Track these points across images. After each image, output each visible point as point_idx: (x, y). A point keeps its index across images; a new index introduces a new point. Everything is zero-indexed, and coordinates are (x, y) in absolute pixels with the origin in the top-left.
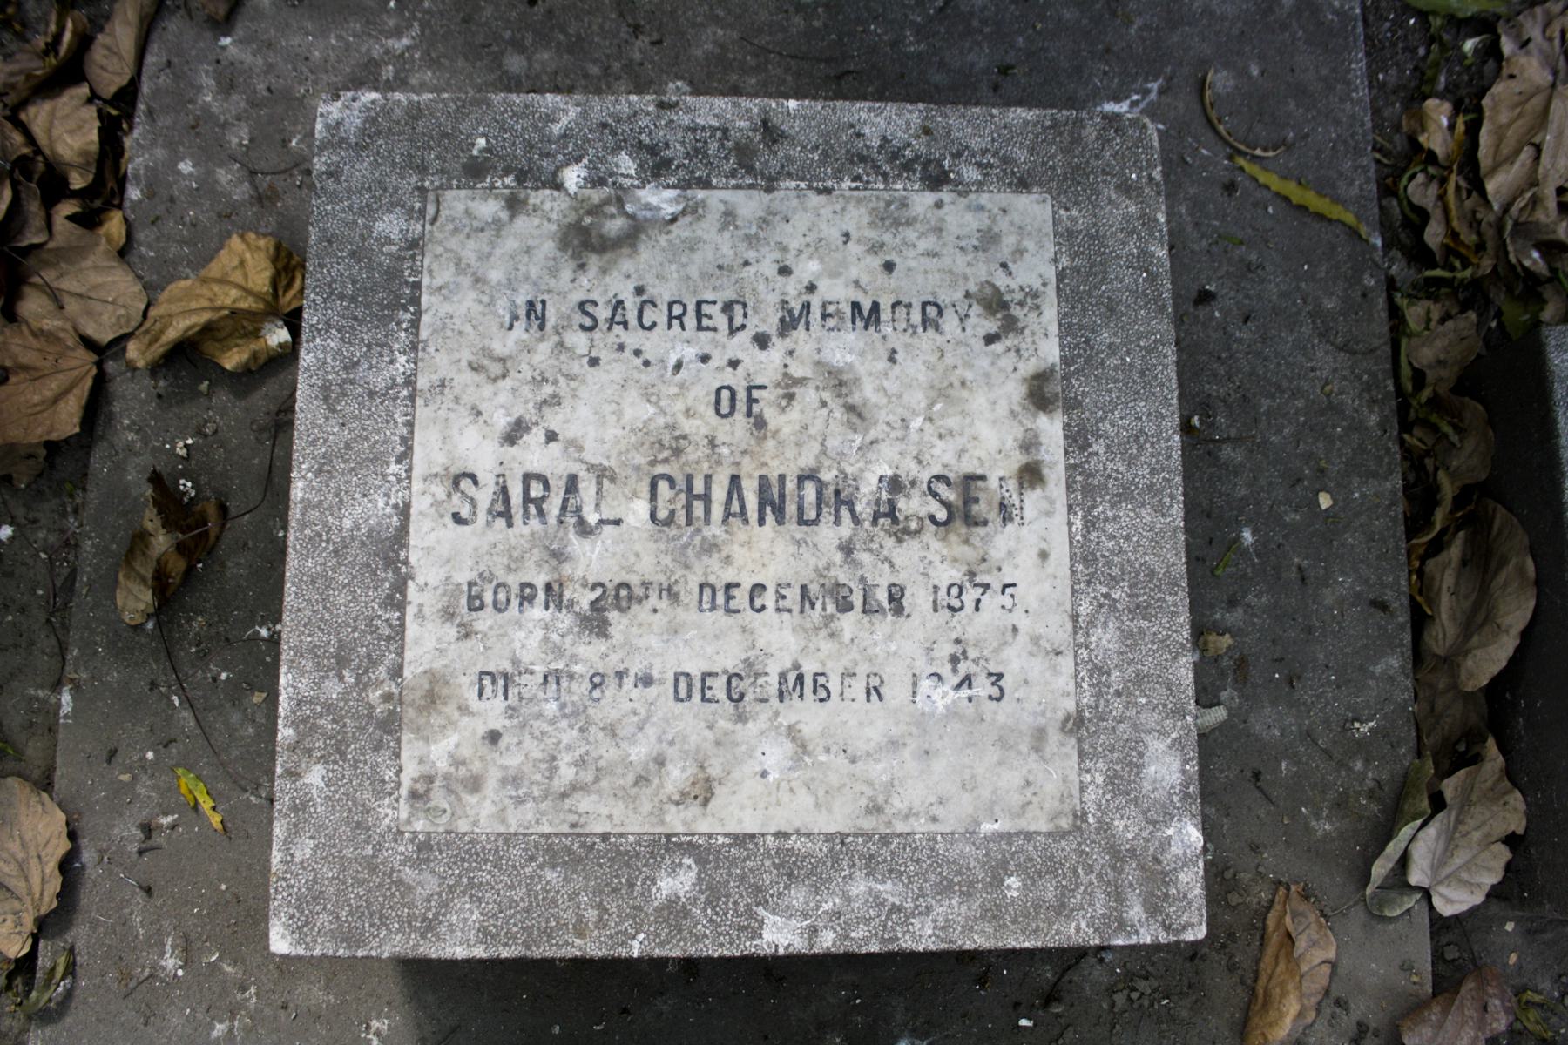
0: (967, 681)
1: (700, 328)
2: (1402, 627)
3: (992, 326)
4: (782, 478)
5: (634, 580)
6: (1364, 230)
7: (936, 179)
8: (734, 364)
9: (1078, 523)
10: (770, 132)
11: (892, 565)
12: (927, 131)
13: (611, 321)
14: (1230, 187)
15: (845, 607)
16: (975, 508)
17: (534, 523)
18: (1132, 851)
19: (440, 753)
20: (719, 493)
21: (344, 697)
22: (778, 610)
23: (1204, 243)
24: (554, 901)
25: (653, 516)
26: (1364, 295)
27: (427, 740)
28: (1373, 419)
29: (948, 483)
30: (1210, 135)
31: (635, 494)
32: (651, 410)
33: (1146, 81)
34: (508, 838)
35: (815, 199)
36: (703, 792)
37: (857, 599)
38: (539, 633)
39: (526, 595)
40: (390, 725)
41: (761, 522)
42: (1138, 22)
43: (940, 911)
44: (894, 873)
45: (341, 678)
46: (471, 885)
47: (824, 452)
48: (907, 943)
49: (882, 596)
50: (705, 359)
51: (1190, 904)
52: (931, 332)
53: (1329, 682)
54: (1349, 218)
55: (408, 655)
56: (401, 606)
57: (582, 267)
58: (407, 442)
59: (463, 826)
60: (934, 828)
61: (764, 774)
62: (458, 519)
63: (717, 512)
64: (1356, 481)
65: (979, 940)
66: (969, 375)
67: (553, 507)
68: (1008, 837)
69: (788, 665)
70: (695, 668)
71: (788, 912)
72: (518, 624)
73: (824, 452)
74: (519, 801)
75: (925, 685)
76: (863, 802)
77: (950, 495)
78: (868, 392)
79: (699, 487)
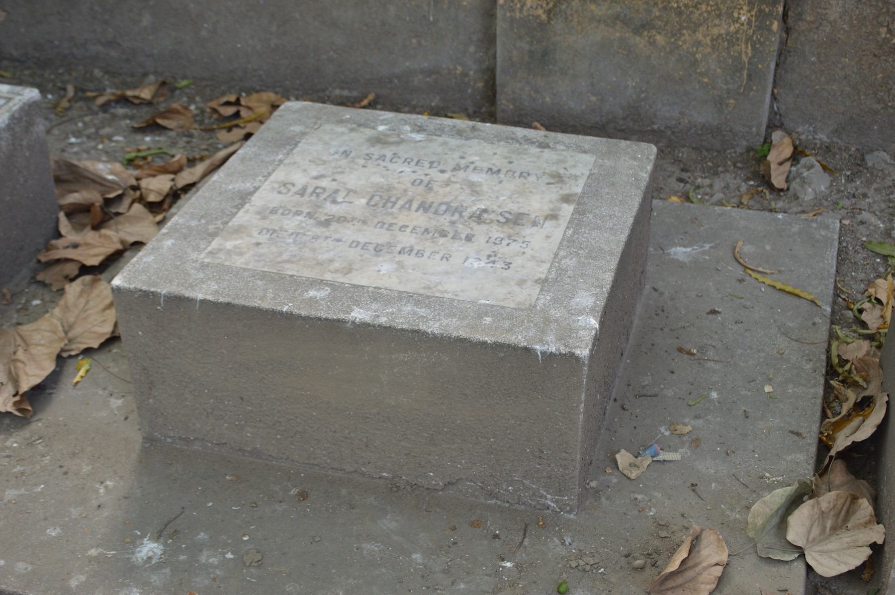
0: (494, 262)
1: (417, 165)
2: (809, 445)
3: (552, 181)
4: (433, 203)
5: (349, 217)
6: (819, 303)
7: (543, 146)
8: (426, 175)
9: (570, 232)
10: (474, 129)
11: (472, 229)
12: (546, 136)
13: (377, 159)
14: (741, 281)
15: (445, 236)
16: (520, 221)
17: (313, 198)
18: (556, 321)
19: (229, 245)
20: (401, 202)
21: (197, 226)
22: (411, 232)
23: (720, 296)
24: (256, 290)
25: (368, 204)
26: (814, 324)
27: (226, 241)
28: (808, 366)
29: (510, 213)
30: (736, 264)
31: (363, 197)
32: (383, 180)
33: (705, 243)
34: (245, 270)
35: (486, 144)
36: (348, 270)
37: (450, 235)
38: (297, 223)
39: (298, 213)
40: (213, 235)
41: (417, 211)
42: (707, 226)
43: (445, 322)
44: (428, 306)
45: (200, 221)
46: (220, 278)
47: (456, 198)
48: (422, 327)
49: (463, 236)
50: (414, 172)
51: (582, 341)
52: (522, 179)
53: (754, 457)
54: (810, 297)
55: (234, 220)
56: (239, 209)
57: (373, 146)
58: (269, 174)
59: (227, 263)
60: (454, 297)
61: (379, 271)
62: (280, 192)
63: (397, 206)
64: (791, 386)
65: (462, 334)
66: (534, 190)
67: (324, 196)
68: (492, 306)
69: (408, 245)
70: (362, 240)
71: (368, 309)
72: (289, 219)
73: (456, 198)
74: (259, 261)
75: (471, 260)
76: (423, 285)
77: (510, 217)
78: (485, 188)
79: (393, 199)
